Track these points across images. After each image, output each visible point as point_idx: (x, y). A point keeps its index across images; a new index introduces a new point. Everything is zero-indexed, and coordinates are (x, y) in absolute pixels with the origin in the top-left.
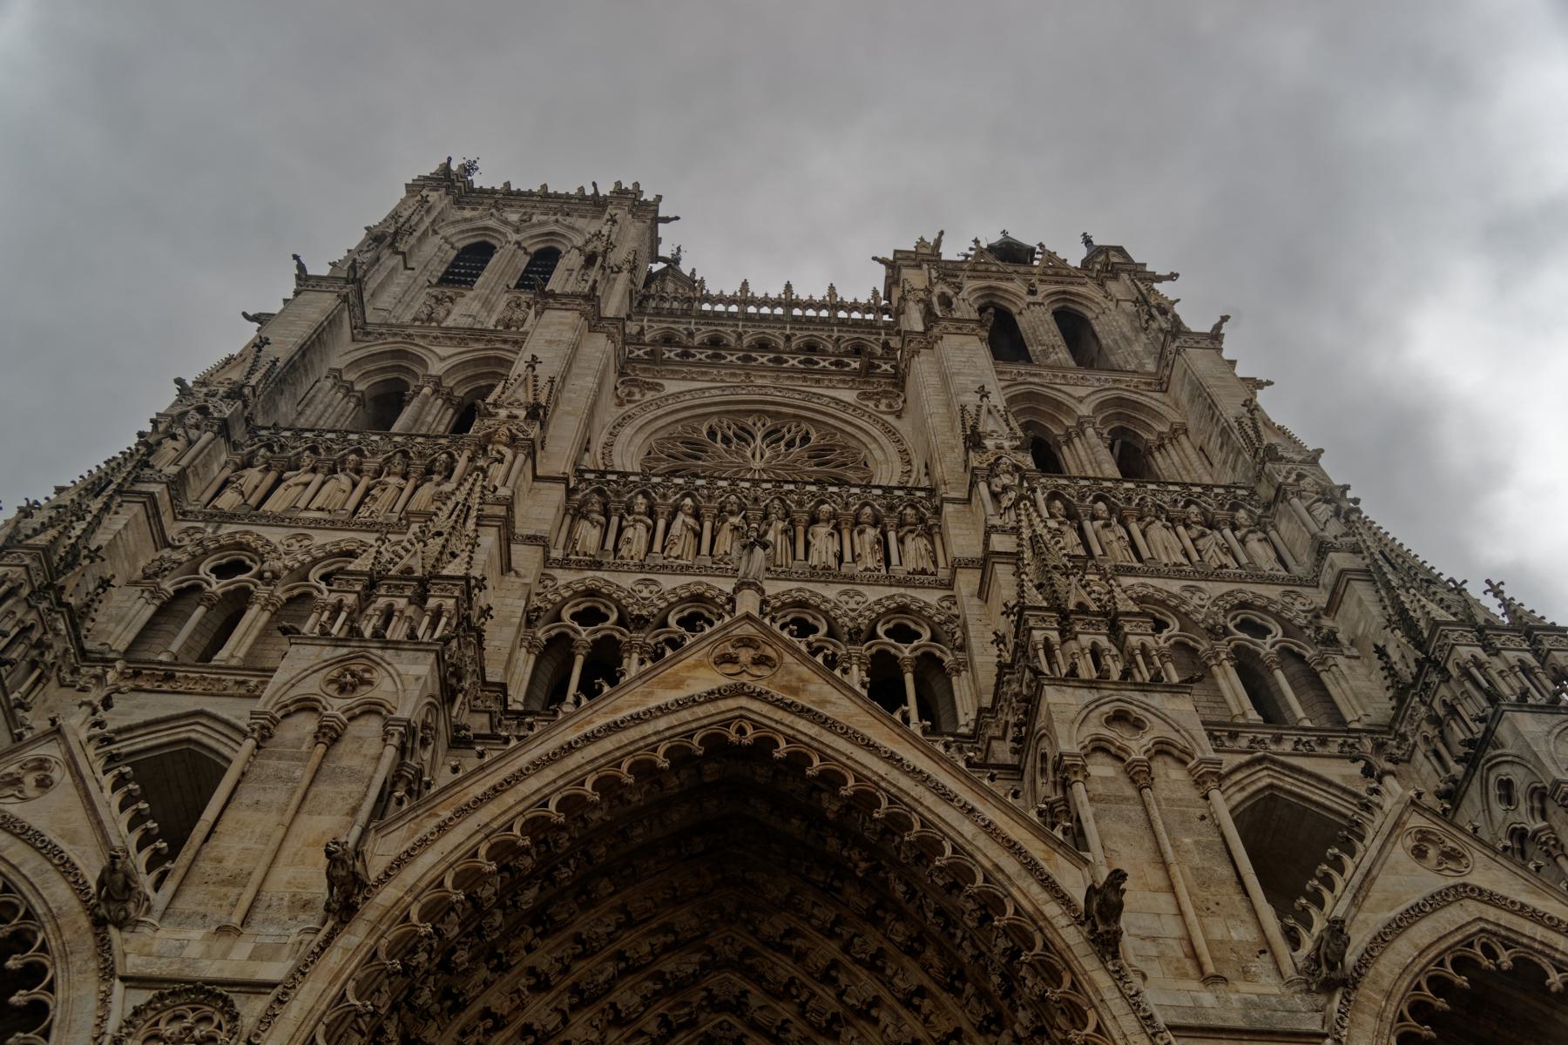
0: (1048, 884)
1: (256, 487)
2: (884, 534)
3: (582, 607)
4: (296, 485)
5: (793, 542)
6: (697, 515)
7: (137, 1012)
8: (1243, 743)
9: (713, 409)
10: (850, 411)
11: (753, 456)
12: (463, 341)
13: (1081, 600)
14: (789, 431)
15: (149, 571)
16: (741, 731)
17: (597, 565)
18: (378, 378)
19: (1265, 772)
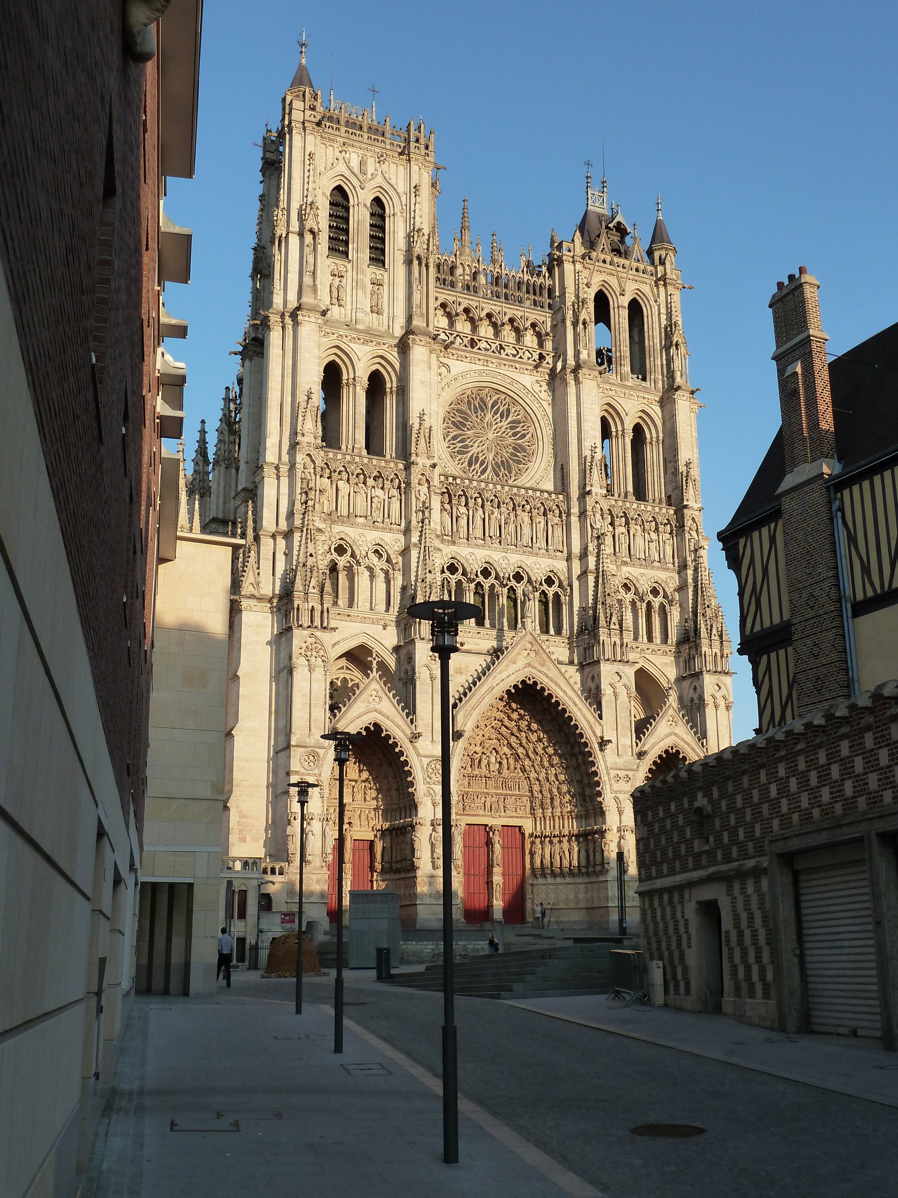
0: (594, 732)
6: (483, 507)
7: (428, 765)
8: (639, 649)
9: (470, 385)
12: (366, 342)
16: (529, 679)
17: (454, 543)
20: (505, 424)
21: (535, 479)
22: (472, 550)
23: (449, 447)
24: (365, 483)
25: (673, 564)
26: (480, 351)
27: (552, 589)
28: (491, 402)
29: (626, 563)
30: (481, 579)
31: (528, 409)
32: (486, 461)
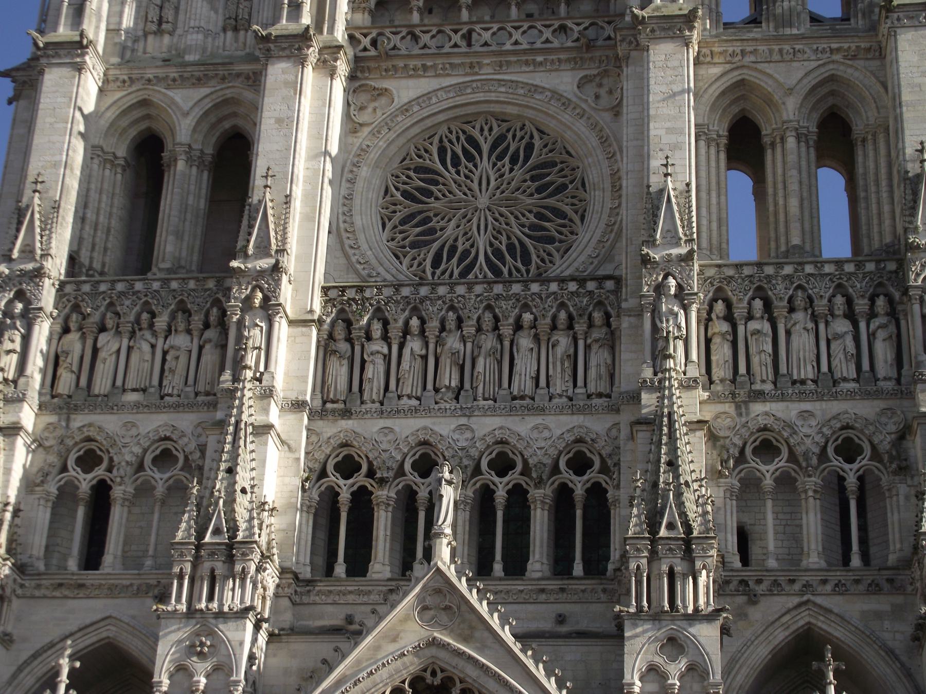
1: (82, 358)
2: (575, 340)
3: (340, 458)
4: (111, 355)
5: (500, 363)
8: (797, 587)
9: (441, 118)
10: (569, 111)
11: (480, 184)
12: (199, 81)
13: (672, 520)
14: (514, 136)
15: (38, 481)
16: (434, 673)
17: (346, 413)
18: (133, 132)
19: (807, 612)
20: (518, 173)
21: (576, 264)
22: (388, 423)
23: (393, 240)
24: (151, 326)
25: (898, 381)
26: (456, 50)
27: (585, 477)
28: (490, 140)
29: (759, 396)
30: (412, 477)
31: (568, 135)
32: (473, 251)
